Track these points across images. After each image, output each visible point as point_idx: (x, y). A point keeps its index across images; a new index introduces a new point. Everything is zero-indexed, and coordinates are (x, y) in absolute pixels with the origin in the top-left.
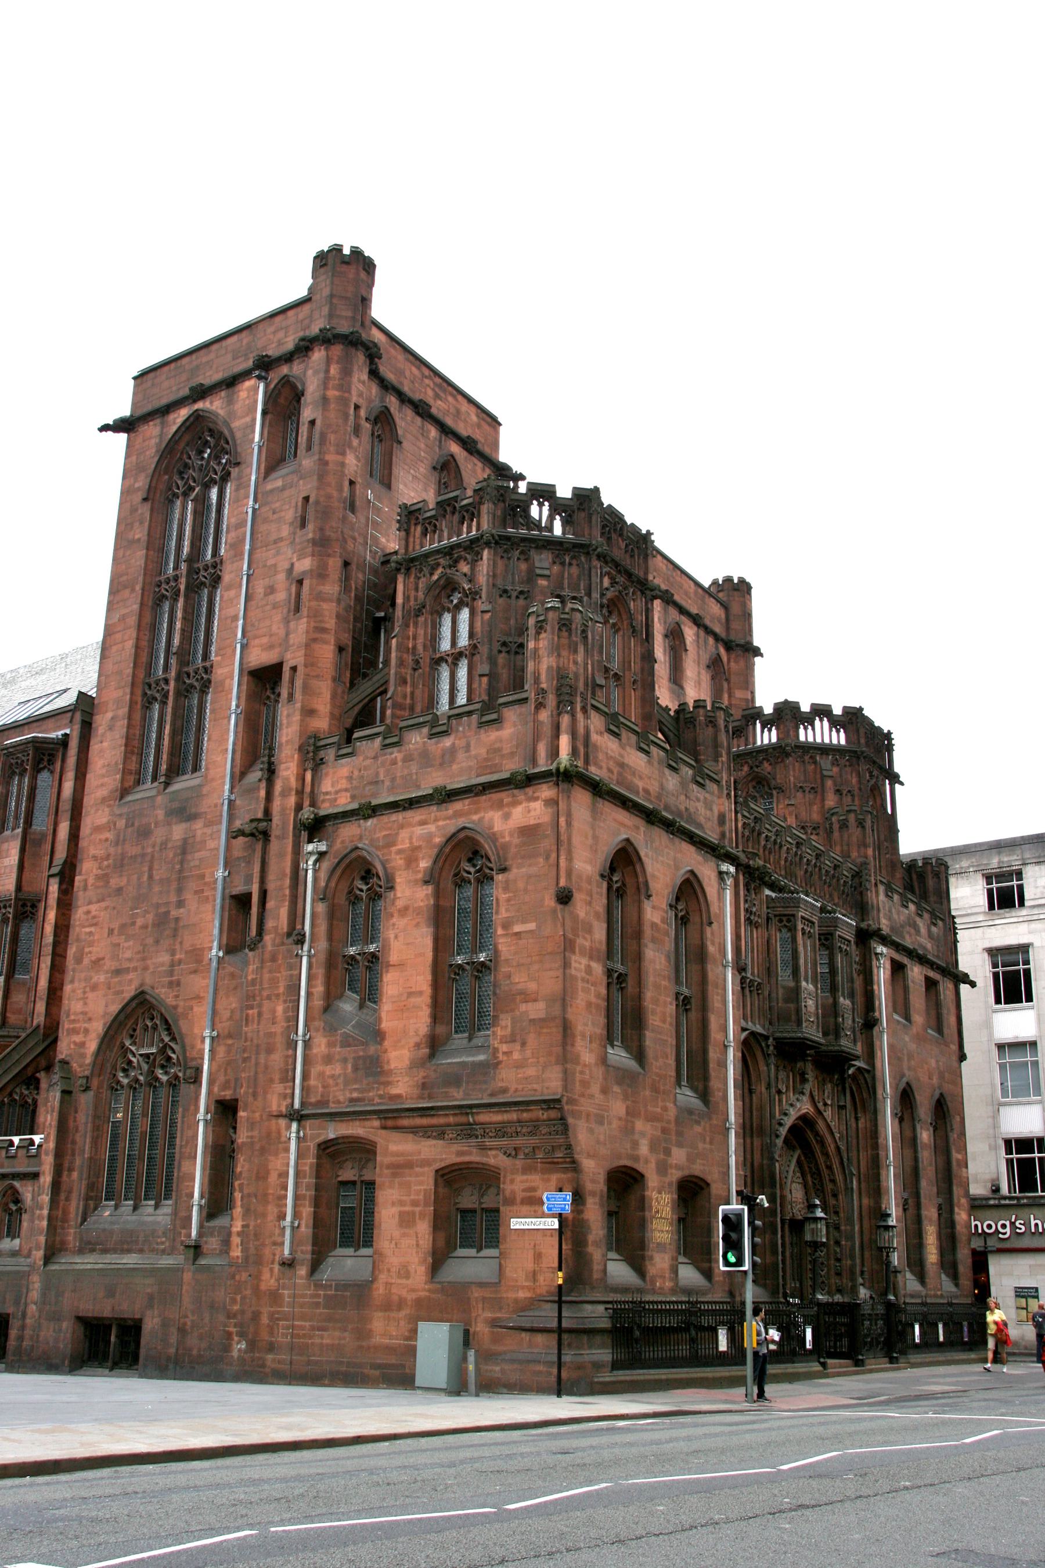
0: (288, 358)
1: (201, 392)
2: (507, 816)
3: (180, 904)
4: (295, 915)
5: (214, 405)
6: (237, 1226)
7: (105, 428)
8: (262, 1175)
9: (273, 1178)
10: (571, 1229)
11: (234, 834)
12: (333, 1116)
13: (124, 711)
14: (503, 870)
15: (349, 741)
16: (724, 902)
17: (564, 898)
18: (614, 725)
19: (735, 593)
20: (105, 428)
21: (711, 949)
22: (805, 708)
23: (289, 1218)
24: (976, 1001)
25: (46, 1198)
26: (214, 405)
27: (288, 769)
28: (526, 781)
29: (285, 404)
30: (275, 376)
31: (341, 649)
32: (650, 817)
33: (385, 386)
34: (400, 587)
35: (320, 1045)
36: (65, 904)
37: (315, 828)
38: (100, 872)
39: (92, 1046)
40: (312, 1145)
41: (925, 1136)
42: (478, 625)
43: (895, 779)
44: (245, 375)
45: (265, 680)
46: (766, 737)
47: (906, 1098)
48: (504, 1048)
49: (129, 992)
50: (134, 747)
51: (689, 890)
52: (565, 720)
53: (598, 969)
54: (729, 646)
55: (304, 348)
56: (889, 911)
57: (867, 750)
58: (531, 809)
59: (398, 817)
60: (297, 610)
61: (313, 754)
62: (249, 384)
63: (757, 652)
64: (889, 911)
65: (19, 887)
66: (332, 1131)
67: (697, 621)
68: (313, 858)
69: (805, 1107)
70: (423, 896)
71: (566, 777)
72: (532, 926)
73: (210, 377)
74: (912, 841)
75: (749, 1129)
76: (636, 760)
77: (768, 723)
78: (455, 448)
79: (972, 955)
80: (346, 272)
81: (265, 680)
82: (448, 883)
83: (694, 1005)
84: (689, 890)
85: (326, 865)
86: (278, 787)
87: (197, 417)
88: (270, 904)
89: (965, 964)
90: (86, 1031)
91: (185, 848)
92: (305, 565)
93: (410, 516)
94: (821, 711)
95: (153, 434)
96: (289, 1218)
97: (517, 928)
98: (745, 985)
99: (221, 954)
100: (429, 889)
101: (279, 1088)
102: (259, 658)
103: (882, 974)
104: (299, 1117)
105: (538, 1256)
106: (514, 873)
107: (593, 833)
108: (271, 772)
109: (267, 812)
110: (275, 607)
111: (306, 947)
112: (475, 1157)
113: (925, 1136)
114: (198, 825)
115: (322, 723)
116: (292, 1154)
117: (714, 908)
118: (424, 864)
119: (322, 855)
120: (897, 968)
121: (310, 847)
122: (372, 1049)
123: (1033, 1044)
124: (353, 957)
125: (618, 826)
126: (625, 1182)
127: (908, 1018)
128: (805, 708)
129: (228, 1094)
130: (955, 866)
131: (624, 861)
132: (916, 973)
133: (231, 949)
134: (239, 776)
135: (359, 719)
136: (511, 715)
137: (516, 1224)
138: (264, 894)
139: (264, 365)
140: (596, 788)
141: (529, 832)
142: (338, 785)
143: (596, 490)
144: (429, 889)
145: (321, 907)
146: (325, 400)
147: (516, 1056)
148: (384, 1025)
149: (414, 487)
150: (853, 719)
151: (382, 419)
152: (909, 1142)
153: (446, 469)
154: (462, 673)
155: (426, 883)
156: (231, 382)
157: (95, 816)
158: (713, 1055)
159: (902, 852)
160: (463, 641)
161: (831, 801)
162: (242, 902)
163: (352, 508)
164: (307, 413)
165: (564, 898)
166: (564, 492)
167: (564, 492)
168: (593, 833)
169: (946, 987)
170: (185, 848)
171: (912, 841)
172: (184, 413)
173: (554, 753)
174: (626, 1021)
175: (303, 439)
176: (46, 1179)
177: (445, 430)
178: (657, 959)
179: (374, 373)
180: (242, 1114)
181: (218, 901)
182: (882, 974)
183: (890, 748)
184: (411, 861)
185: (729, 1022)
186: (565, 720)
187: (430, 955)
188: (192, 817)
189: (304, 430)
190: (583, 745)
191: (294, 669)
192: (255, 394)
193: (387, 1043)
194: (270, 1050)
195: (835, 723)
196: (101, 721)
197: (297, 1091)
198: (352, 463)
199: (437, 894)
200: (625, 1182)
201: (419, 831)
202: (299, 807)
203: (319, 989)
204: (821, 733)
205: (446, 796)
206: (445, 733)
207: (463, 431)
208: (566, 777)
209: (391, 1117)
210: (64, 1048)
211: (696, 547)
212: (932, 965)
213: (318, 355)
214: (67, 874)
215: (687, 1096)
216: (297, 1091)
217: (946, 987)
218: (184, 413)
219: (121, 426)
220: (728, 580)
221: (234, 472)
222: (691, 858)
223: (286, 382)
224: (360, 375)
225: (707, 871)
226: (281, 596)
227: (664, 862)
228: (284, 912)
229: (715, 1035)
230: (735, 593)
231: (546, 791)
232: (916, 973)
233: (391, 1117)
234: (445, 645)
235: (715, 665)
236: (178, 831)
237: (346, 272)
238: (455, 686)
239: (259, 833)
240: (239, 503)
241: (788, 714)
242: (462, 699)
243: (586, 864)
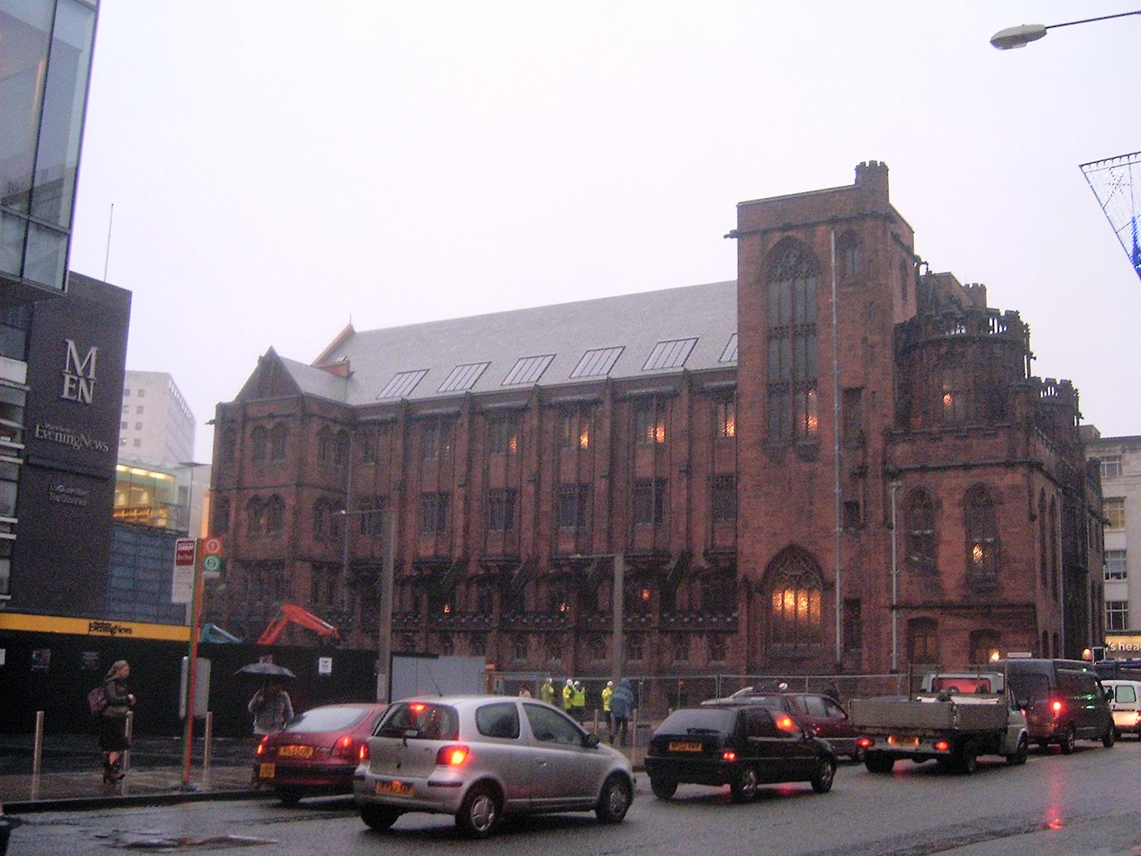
0: (848, 220)
2: (1002, 479)
3: (811, 504)
4: (887, 517)
6: (865, 656)
7: (726, 237)
8: (878, 635)
9: (884, 635)
12: (915, 608)
14: (1001, 504)
20: (726, 237)
23: (894, 652)
26: (800, 236)
27: (876, 443)
28: (1009, 465)
38: (754, 483)
40: (904, 621)
48: (1005, 581)
49: (783, 543)
58: (1015, 478)
61: (890, 438)
62: (822, 228)
66: (914, 615)
68: (894, 489)
70: (958, 512)
80: (873, 177)
81: (851, 394)
82: (969, 507)
85: (901, 492)
86: (870, 451)
90: (756, 563)
91: (811, 477)
96: (894, 652)
99: (841, 530)
102: (847, 382)
104: (892, 608)
106: (1007, 505)
111: (894, 530)
112: (990, 626)
114: (818, 464)
115: (890, 421)
116: (895, 623)
119: (898, 488)
123: (1125, 552)
124: (917, 536)
129: (852, 596)
139: (833, 221)
141: (1015, 488)
147: (1012, 585)
148: (941, 568)
162: (851, 508)
170: (811, 477)
176: (743, 632)
180: (863, 606)
181: (837, 505)
188: (814, 460)
193: (943, 577)
194: (878, 577)
197: (894, 597)
202: (884, 463)
205: (967, 467)
209: (947, 608)
210: (742, 569)
216: (894, 597)
219: (733, 235)
223: (850, 233)
231: (1022, 470)
233: (947, 608)
236: (806, 467)
237: (873, 177)
239: (861, 473)
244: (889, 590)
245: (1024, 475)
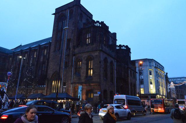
0: (72, 7)
1: (62, 11)
2: (94, 54)
5: (64, 12)
7: (52, 14)
10: (100, 95)
11: (66, 56)
13: (54, 43)
15: (78, 46)
16: (115, 64)
17: (100, 62)
18: (105, 45)
19: (115, 34)
20: (52, 14)
21: (114, 68)
22: (122, 45)
24: (138, 75)
25: (46, 92)
29: (71, 13)
30: (70, 9)
31: (77, 37)
32: (108, 54)
33: (82, 11)
34: (83, 31)
35: (74, 77)
36: (48, 63)
37: (74, 55)
39: (51, 77)
41: (133, 88)
42: (91, 35)
43: (131, 53)
44: (67, 9)
45: (69, 41)
46: (118, 48)
47: (131, 84)
50: (55, 47)
51: (111, 62)
52: (100, 44)
53: (103, 70)
54: (114, 39)
55: (73, 6)
56: (130, 66)
57: (128, 49)
58: (97, 53)
59: (83, 54)
60: (73, 33)
61: (74, 48)
63: (117, 40)
64: (130, 66)
65: (43, 61)
67: (111, 37)
69: (122, 84)
71: (101, 50)
72: (96, 65)
73: (64, 9)
74: (132, 59)
75: (117, 86)
76: (107, 49)
77: (118, 47)
78: (88, 18)
79: (137, 71)
83: (112, 73)
84: (111, 62)
86: (70, 51)
87: (62, 13)
88: (69, 63)
89: (137, 71)
92: (73, 28)
93: (84, 24)
94: (124, 46)
95: (57, 15)
97: (95, 65)
98: (117, 72)
100: (86, 61)
101: (70, 81)
102: (68, 38)
103: (129, 72)
105: (96, 98)
107: (103, 56)
108: (70, 49)
109: (69, 54)
110: (70, 33)
113: (133, 88)
117: (114, 64)
118: (85, 59)
120: (131, 71)
121: (74, 57)
122: (80, 77)
125: (105, 55)
126: (105, 91)
127: (131, 76)
128: (122, 45)
130: (136, 62)
131: (105, 60)
132: (132, 72)
133: (66, 67)
134: (66, 50)
135: (78, 45)
136: (94, 44)
137: (94, 95)
138: (69, 62)
139: (69, 8)
140: (103, 52)
141: (96, 56)
142: (76, 51)
143: (103, 22)
144: (86, 61)
145: (75, 63)
146: (75, 12)
148: (81, 75)
149: (84, 21)
150: (127, 47)
151: (81, 14)
152: (131, 88)
153: (87, 20)
154: (90, 39)
155: (86, 60)
156: (66, 10)
157: (51, 53)
158: (114, 79)
159: (131, 60)
160: (90, 37)
161: (124, 55)
163: (78, 23)
164: (74, 13)
165: (100, 62)
166: (100, 22)
167: (100, 22)
168: (103, 56)
169: (135, 73)
171: (132, 59)
172: (61, 13)
173: (99, 48)
174: (106, 76)
175: (73, 16)
176: (46, 90)
177: (87, 16)
178: (109, 69)
179: (80, 9)
180: (66, 84)
182: (129, 72)
183: (130, 50)
184: (84, 58)
185: (115, 75)
186: (100, 44)
187: (86, 68)
189: (73, 14)
190: (102, 47)
191: (72, 39)
192: (68, 11)
195: (125, 47)
196: (52, 44)
198: (78, 18)
199: (87, 62)
200: (105, 91)
201: (85, 55)
203: (74, 71)
204: (124, 48)
206: (88, 46)
207: (89, 16)
208: (101, 50)
210: (48, 77)
211: (111, 30)
212: (134, 71)
213: (75, 7)
214: (48, 59)
215: (112, 83)
217: (135, 73)
218: (61, 13)
219: (54, 14)
220: (114, 33)
221: (66, 19)
222: (112, 59)
224: (79, 9)
225: (113, 60)
226: (71, 32)
227: (109, 60)
228: (71, 64)
229: (114, 77)
230: (115, 34)
232: (132, 72)
234: (87, 37)
235: (112, 41)
238: (88, 41)
240: (67, 22)
241: (120, 46)
242: (89, 42)
243: (102, 59)
244: (71, 80)
245: (98, 53)
